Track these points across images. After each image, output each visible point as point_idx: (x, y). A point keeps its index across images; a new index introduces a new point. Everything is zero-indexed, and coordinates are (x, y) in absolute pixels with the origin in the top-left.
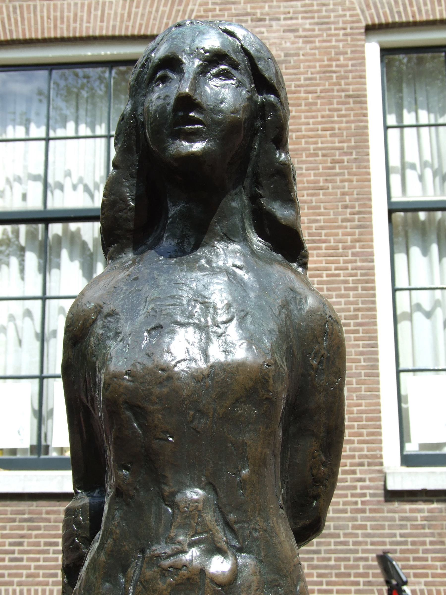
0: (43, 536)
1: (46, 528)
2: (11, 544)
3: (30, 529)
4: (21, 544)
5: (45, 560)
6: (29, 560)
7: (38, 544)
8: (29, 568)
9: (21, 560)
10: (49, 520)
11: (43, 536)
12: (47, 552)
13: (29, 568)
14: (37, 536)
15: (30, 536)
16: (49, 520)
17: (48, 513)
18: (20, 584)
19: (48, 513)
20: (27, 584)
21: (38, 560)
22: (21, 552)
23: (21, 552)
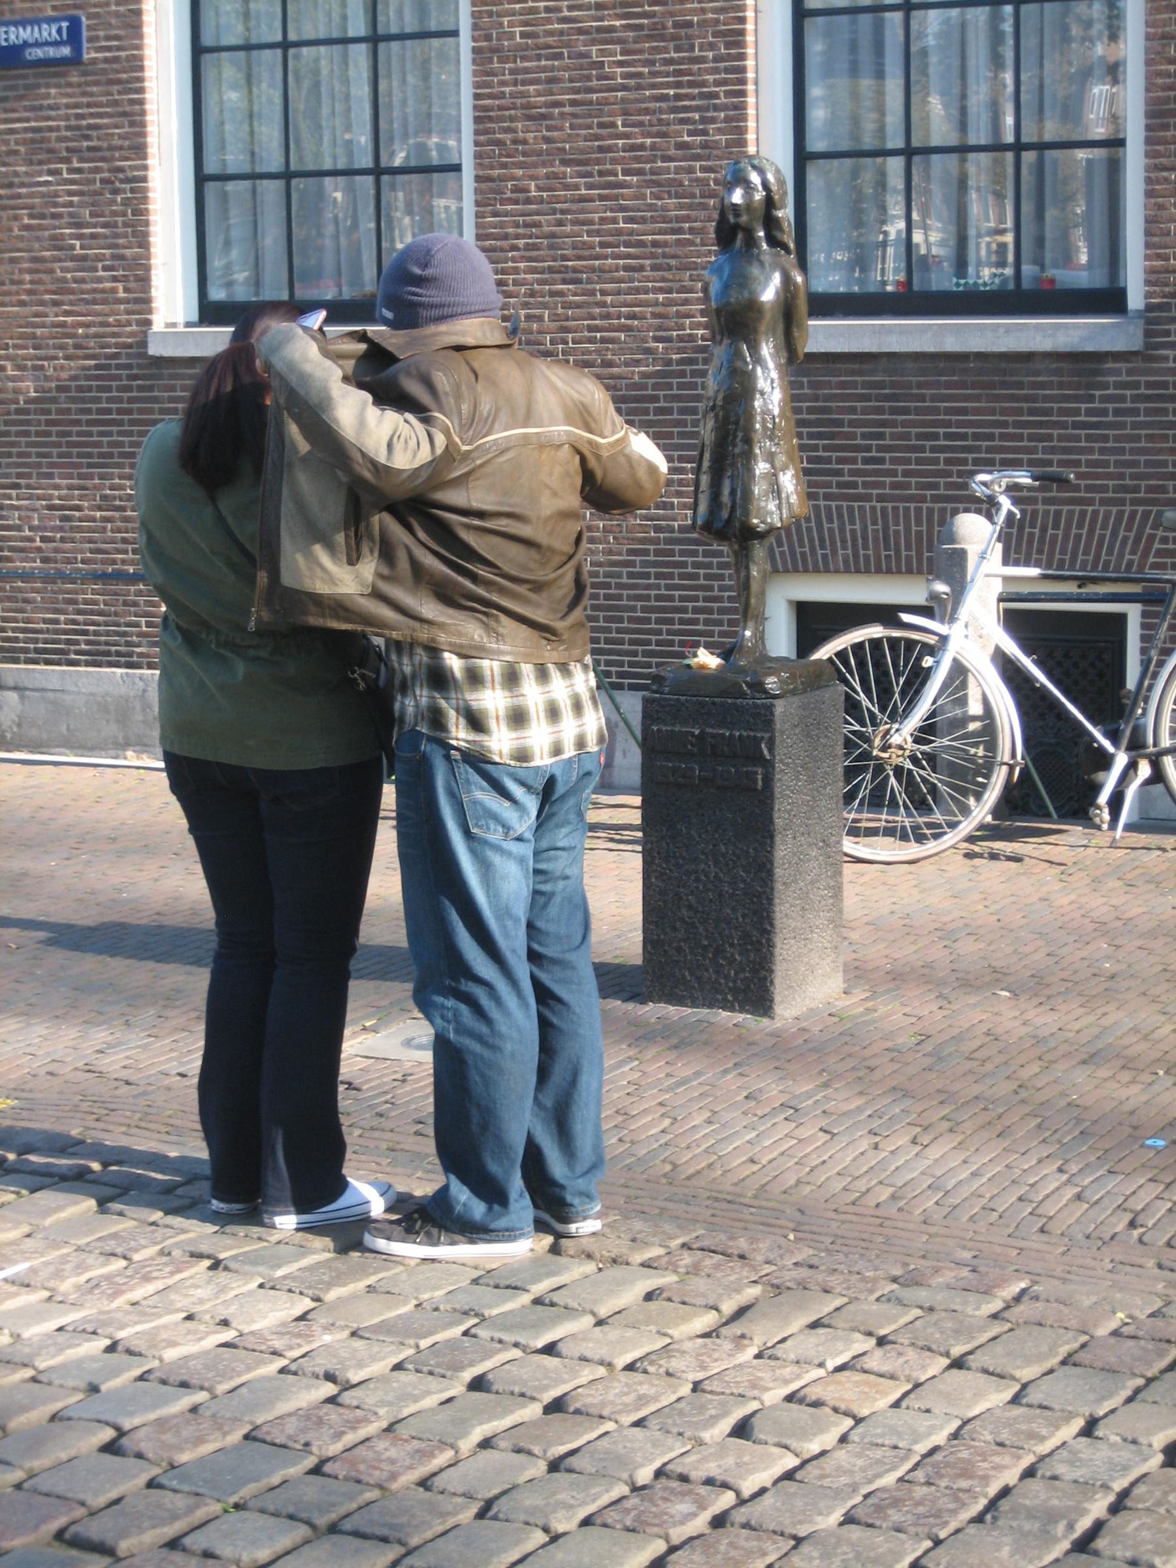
0: (914, 424)
1: (918, 411)
2: (864, 436)
3: (893, 411)
4: (880, 436)
5: (919, 461)
6: (894, 461)
7: (907, 436)
8: (894, 473)
9: (881, 461)
10: (922, 398)
11: (914, 424)
12: (921, 449)
13: (894, 473)
14: (905, 424)
15: (893, 424)
16: (922, 398)
17: (920, 385)
18: (881, 498)
19: (920, 385)
20: (892, 499)
21: (907, 461)
22: (880, 449)
23: (880, 449)
